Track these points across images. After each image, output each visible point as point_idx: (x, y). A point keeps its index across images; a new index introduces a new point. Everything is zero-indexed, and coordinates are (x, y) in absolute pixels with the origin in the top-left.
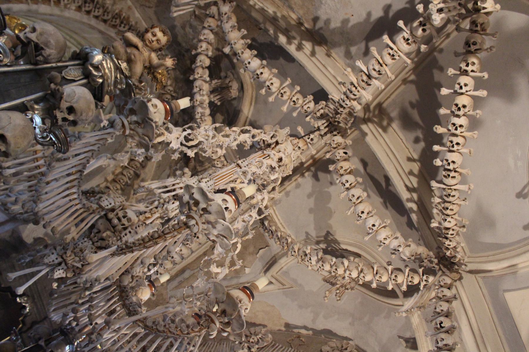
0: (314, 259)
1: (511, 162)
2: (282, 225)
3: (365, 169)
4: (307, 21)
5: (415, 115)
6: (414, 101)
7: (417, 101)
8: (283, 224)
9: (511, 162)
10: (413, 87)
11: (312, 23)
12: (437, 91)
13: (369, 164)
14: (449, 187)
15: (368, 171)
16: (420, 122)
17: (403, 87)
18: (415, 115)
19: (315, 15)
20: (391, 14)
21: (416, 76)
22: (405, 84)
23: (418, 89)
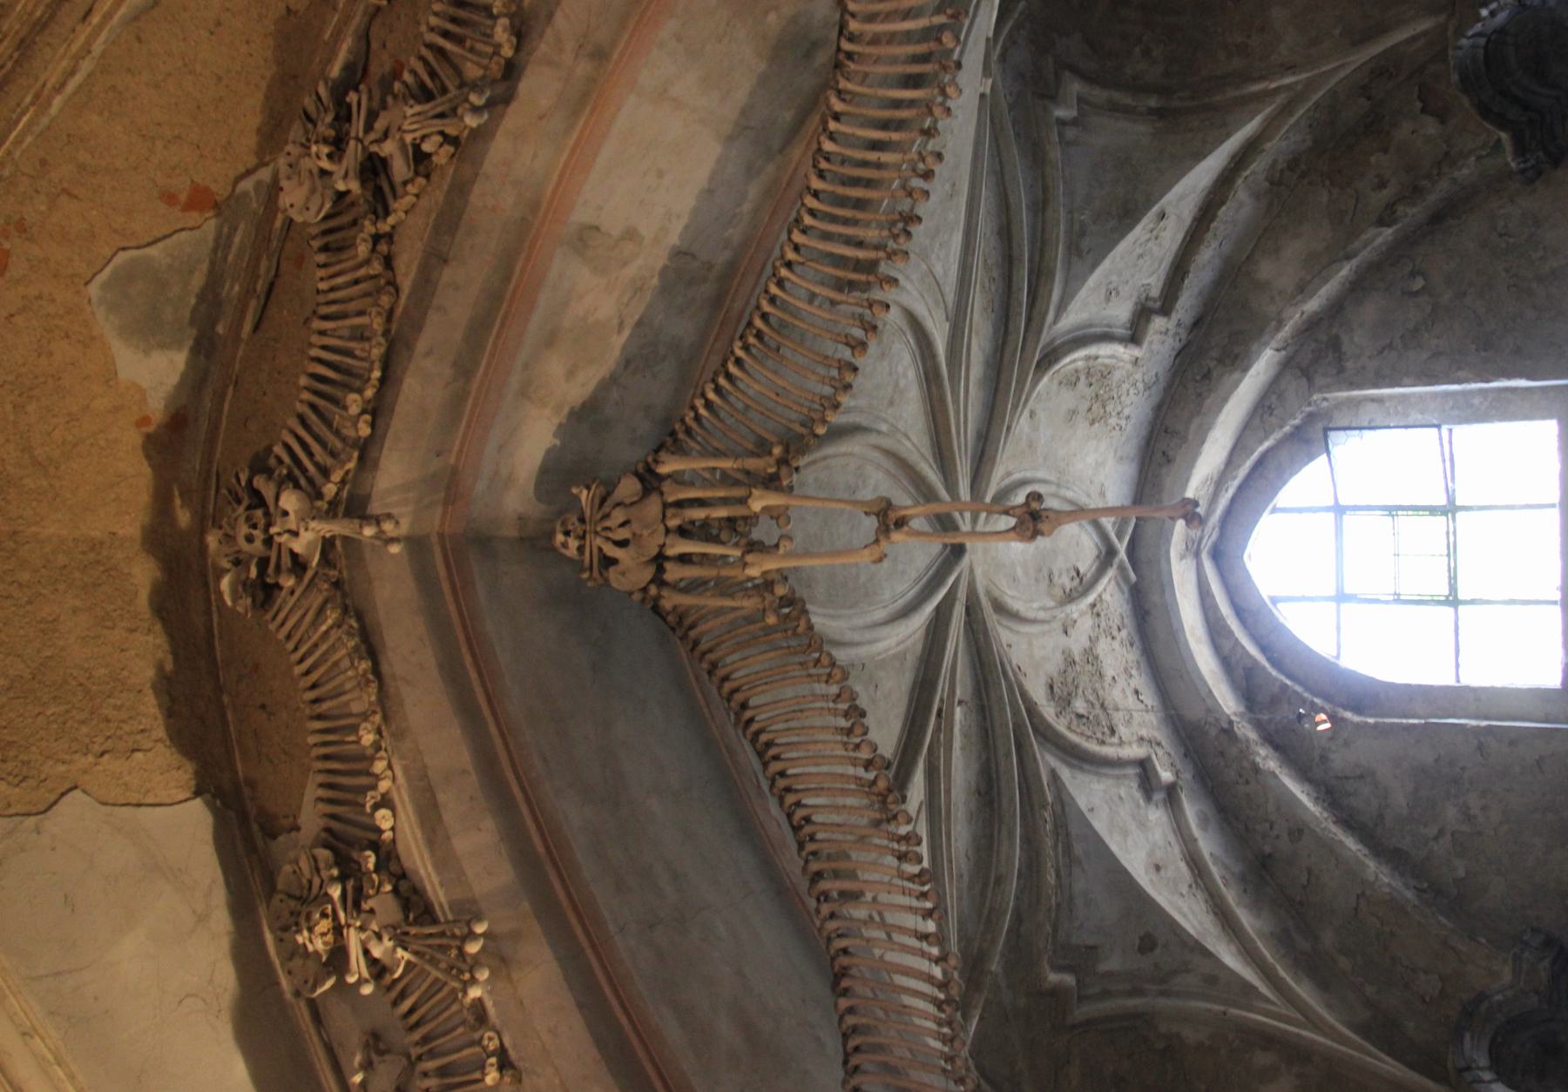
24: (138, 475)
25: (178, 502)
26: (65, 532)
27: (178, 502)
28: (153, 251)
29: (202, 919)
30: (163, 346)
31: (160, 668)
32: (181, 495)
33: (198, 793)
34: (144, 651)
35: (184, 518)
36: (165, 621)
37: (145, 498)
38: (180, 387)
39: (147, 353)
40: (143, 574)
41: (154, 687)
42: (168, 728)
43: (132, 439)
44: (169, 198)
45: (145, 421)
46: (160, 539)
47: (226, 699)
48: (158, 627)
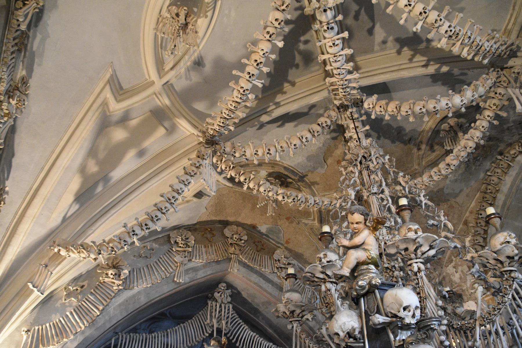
0: (443, 30)
1: (233, 14)
2: (514, 7)
3: (373, 27)
4: (341, 141)
5: (298, 59)
6: (294, 69)
7: (292, 68)
8: (512, 8)
9: (233, 14)
10: (290, 78)
11: (339, 138)
12: (273, 71)
13: (366, 29)
15: (371, 24)
16: (296, 53)
17: (297, 81)
18: (298, 59)
19: (333, 141)
20: (280, 123)
28: (282, 235)
44: (289, 239)
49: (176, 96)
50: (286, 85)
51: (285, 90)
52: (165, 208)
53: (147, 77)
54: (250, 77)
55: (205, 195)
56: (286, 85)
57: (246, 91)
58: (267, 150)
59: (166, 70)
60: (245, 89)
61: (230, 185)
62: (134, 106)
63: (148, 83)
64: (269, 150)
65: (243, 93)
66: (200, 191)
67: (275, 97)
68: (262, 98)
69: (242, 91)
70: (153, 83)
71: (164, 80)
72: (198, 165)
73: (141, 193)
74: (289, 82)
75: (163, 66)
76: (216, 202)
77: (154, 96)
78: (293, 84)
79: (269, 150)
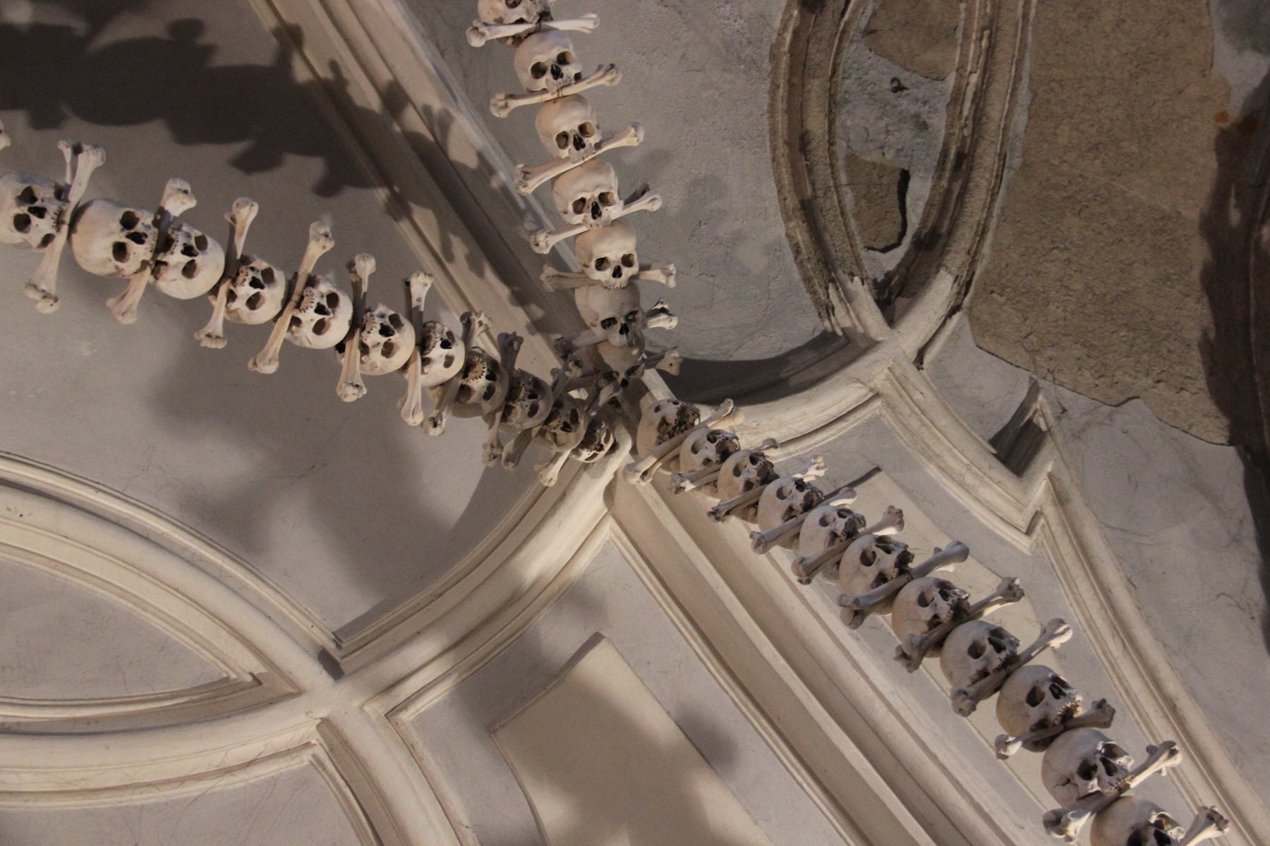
14: (67, 218)
21: (303, 91)
22: (277, 33)
23: (246, 76)
24: (1208, 164)
25: (1233, 201)
26: (1143, 197)
27: (1233, 201)
29: (1236, 540)
30: (1256, 48)
31: (1205, 333)
32: (1237, 195)
33: (1231, 443)
34: (1195, 316)
35: (1235, 217)
36: (1211, 299)
37: (1207, 189)
38: (1258, 92)
39: (1240, 51)
40: (1199, 253)
41: (1200, 346)
42: (1209, 383)
43: (1207, 132)
45: (1222, 116)
46: (1212, 226)
47: (1257, 378)
48: (1205, 300)
49: (400, 610)
50: (301, 74)
51: (324, 73)
52: (923, 601)
53: (306, 757)
54: (41, 212)
55: (1023, 409)
56: (301, 74)
57: (139, 228)
58: (542, 83)
59: (257, 667)
60: (122, 238)
61: (942, 288)
62: (462, 816)
63: (331, 751)
64: (538, 71)
65: (151, 242)
66: (994, 442)
67: (367, 113)
68: (387, 182)
69: (141, 253)
70: (326, 725)
71: (310, 672)
72: (710, 451)
73: (933, 757)
74: (283, 63)
75: (238, 686)
76: (1078, 351)
77: (407, 716)
78: (290, 37)
79: (538, 71)
